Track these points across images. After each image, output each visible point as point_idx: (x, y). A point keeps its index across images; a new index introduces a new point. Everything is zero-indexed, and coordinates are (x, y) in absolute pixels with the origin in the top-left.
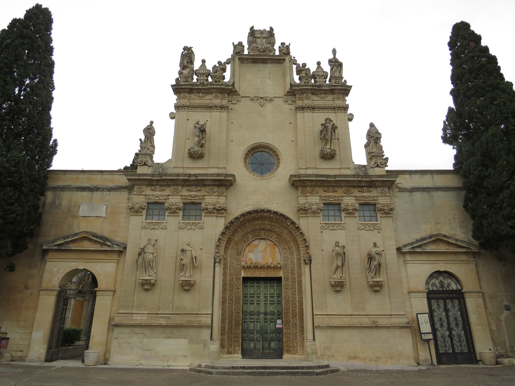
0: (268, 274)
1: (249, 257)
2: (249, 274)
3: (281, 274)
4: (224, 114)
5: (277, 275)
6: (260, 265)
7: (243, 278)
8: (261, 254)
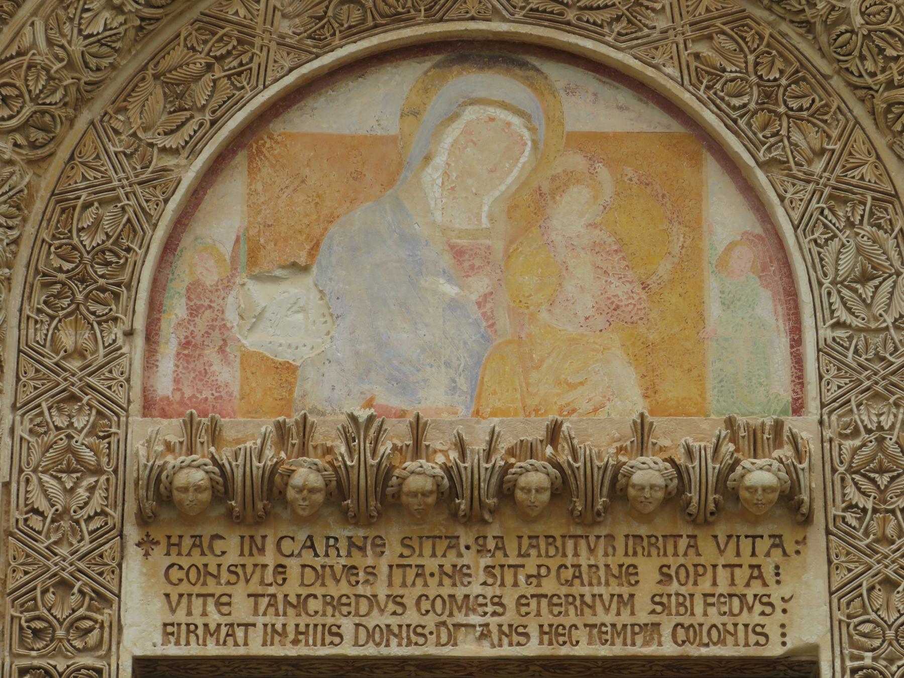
0: (584, 605)
1: (252, 342)
2: (241, 610)
5: (722, 635)
6: (434, 465)
8: (451, 290)
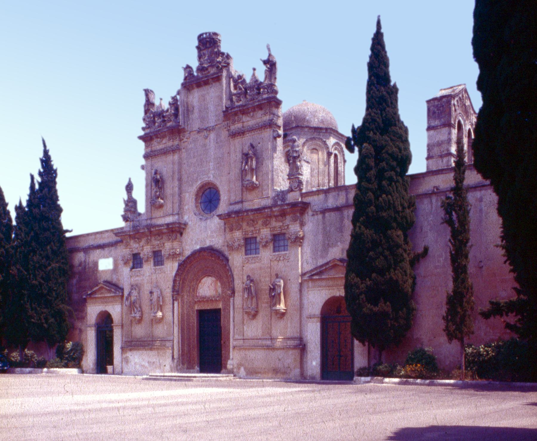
3: (220, 306)
4: (176, 157)
7: (197, 310)
